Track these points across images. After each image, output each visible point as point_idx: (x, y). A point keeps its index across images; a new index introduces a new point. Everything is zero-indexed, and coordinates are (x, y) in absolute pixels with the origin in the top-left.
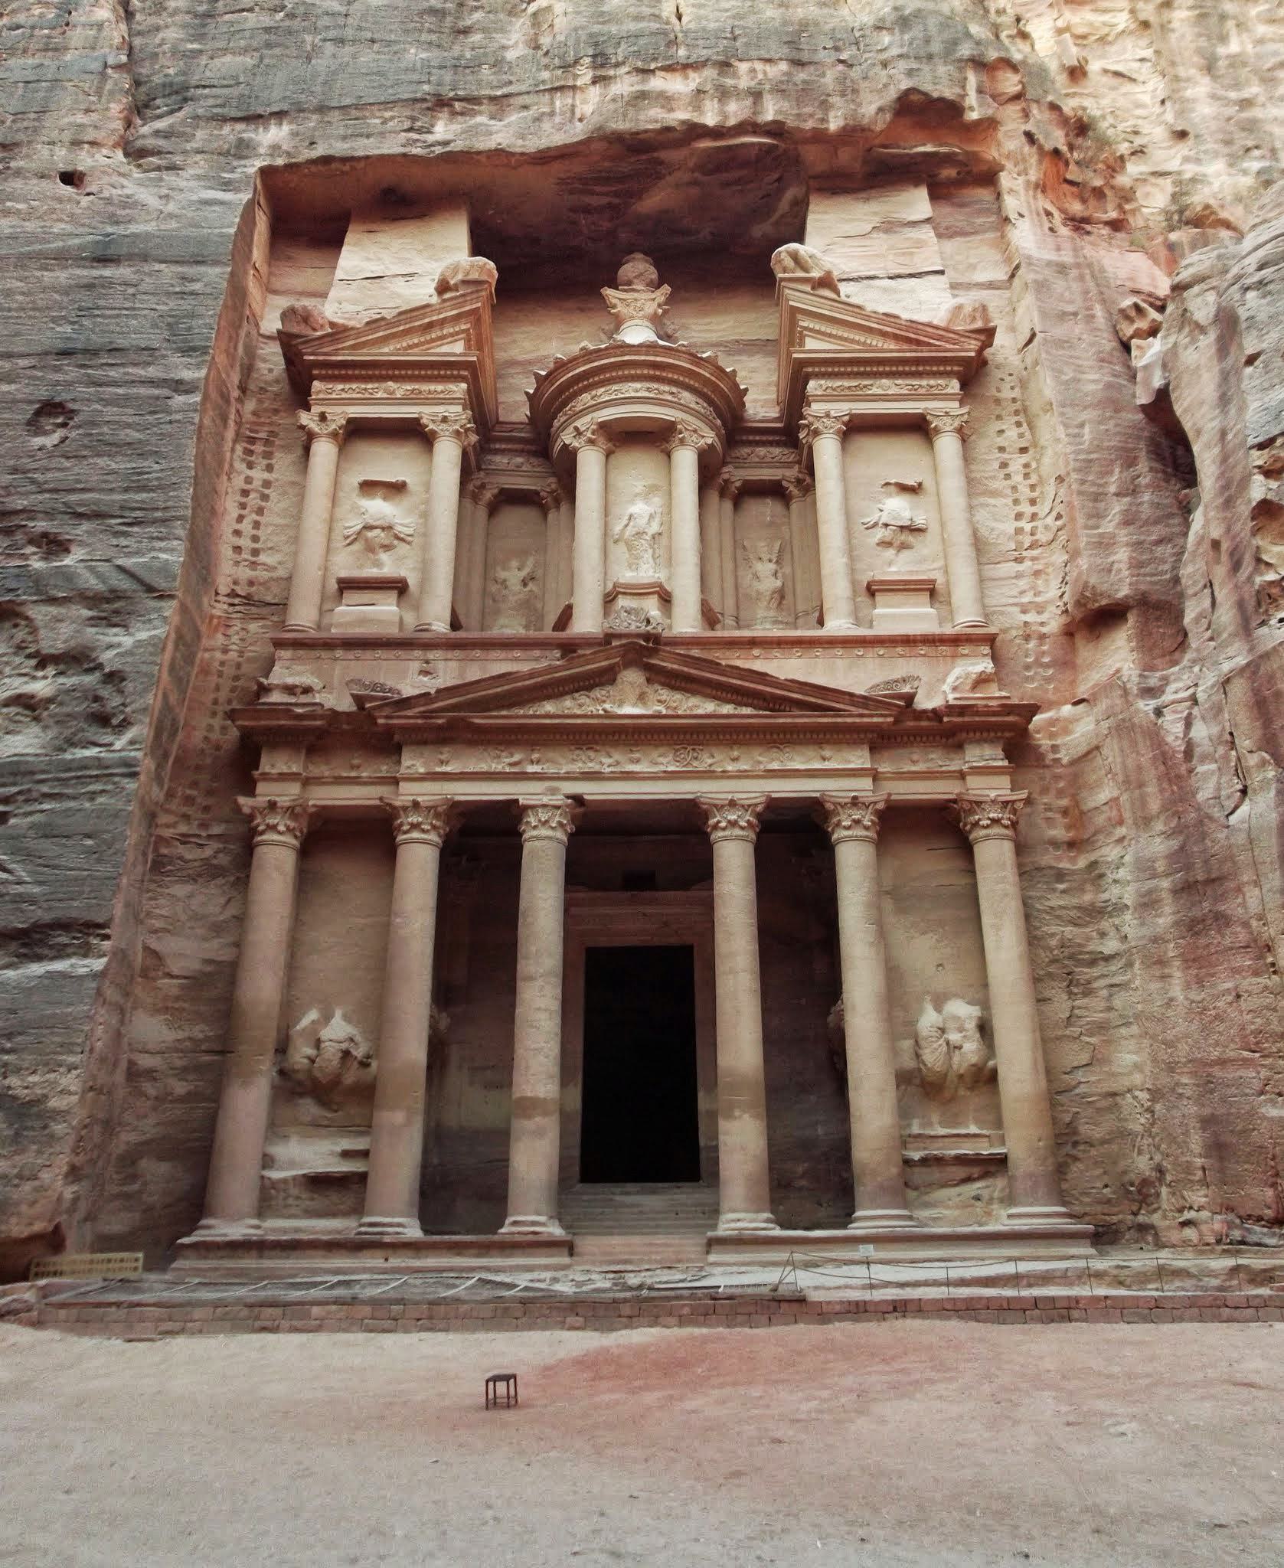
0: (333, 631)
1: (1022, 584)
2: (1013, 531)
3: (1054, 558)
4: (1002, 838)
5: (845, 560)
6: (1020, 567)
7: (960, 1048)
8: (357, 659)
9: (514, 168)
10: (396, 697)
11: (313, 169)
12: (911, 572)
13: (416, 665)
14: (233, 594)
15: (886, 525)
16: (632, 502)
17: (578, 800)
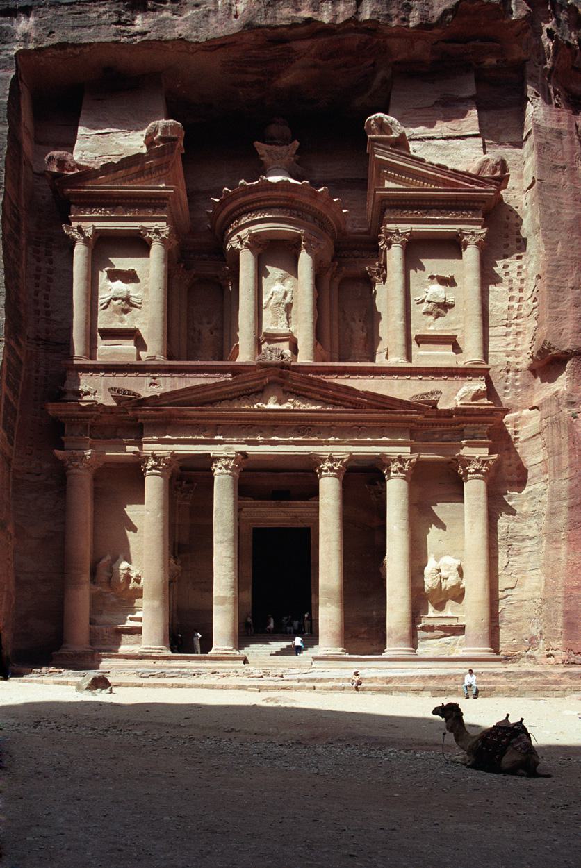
0: (98, 359)
1: (509, 339)
2: (507, 308)
3: (528, 325)
4: (479, 478)
5: (402, 322)
6: (509, 330)
7: (447, 579)
8: (114, 376)
9: (193, 53)
10: (138, 398)
11: (55, 52)
12: (442, 331)
13: (149, 380)
14: (37, 339)
15: (429, 302)
16: (273, 284)
17: (244, 454)
